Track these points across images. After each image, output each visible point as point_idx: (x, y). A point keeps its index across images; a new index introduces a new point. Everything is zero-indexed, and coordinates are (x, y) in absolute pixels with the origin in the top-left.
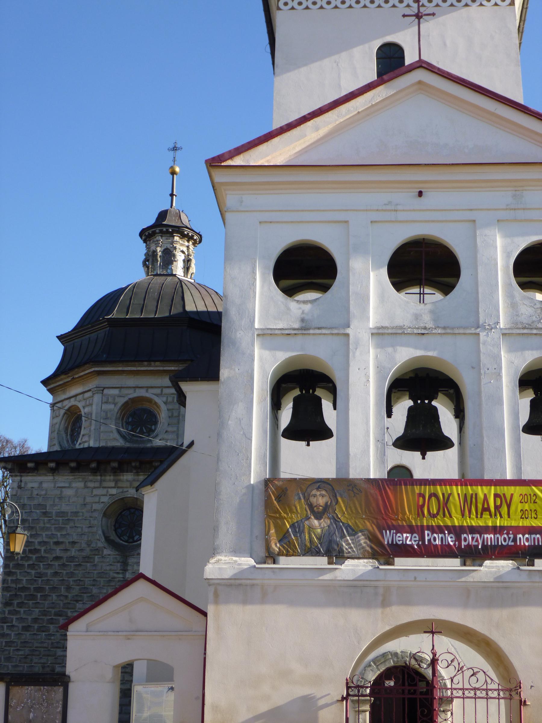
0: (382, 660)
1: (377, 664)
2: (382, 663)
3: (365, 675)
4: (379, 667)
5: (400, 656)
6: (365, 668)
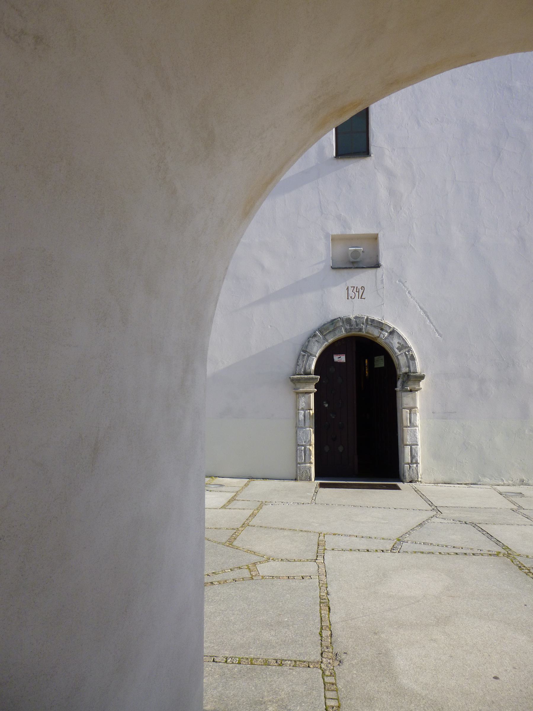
0: (331, 329)
1: (324, 334)
2: (330, 332)
3: (309, 347)
4: (327, 337)
5: (354, 323)
6: (308, 338)
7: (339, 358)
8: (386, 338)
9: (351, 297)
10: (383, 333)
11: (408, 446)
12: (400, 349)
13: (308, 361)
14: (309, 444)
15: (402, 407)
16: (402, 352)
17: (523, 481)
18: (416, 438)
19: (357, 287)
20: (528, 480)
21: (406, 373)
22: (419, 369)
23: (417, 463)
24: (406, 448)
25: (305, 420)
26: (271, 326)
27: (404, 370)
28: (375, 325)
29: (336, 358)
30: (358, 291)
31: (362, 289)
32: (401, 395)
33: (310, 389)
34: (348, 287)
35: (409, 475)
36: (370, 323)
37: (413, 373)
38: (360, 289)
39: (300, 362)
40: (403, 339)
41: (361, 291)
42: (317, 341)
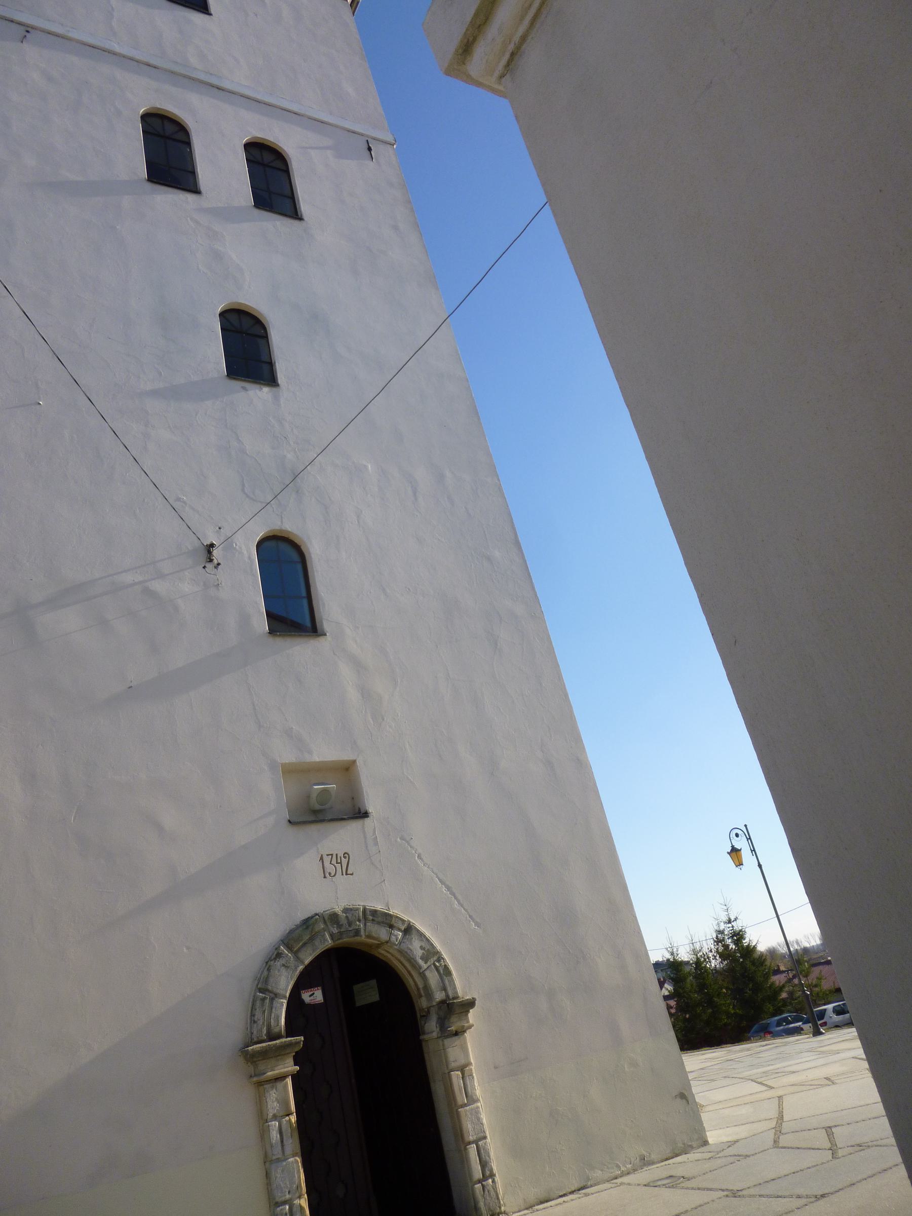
0: (306, 937)
1: (295, 949)
2: (304, 944)
3: (271, 980)
4: (301, 955)
5: (343, 921)
7: (310, 996)
8: (400, 943)
9: (330, 874)
10: (395, 934)
11: (472, 1145)
12: (425, 959)
13: (274, 1010)
14: (297, 1195)
15: (447, 1068)
16: (429, 963)
17: (644, 1159)
18: (482, 1124)
19: (337, 855)
20: (650, 1154)
21: (443, 1002)
22: (462, 988)
23: (492, 1175)
24: (470, 1149)
25: (282, 1141)
26: (188, 948)
27: (439, 996)
28: (380, 919)
29: (306, 997)
31: (345, 857)
32: (443, 1045)
33: (286, 1070)
34: (322, 855)
35: (485, 1205)
36: (371, 918)
37: (454, 998)
40: (428, 940)
41: (344, 861)
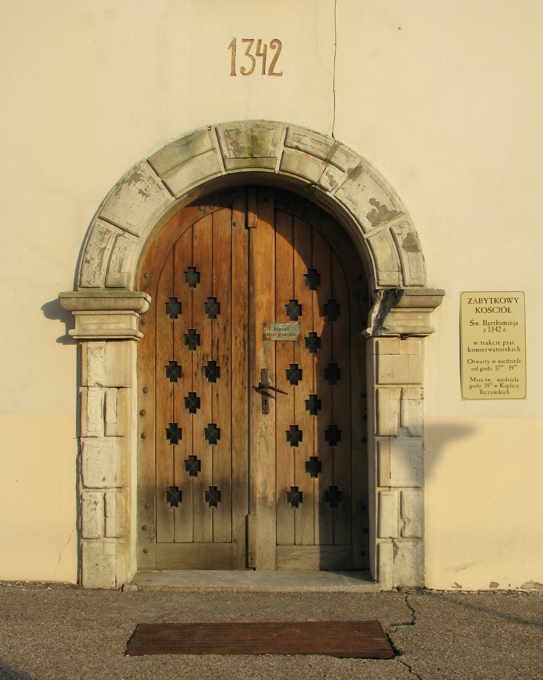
10: (331, 173)
30: (262, 52)
38: (268, 47)
39: (93, 253)
41: (271, 54)
42: (141, 192)
